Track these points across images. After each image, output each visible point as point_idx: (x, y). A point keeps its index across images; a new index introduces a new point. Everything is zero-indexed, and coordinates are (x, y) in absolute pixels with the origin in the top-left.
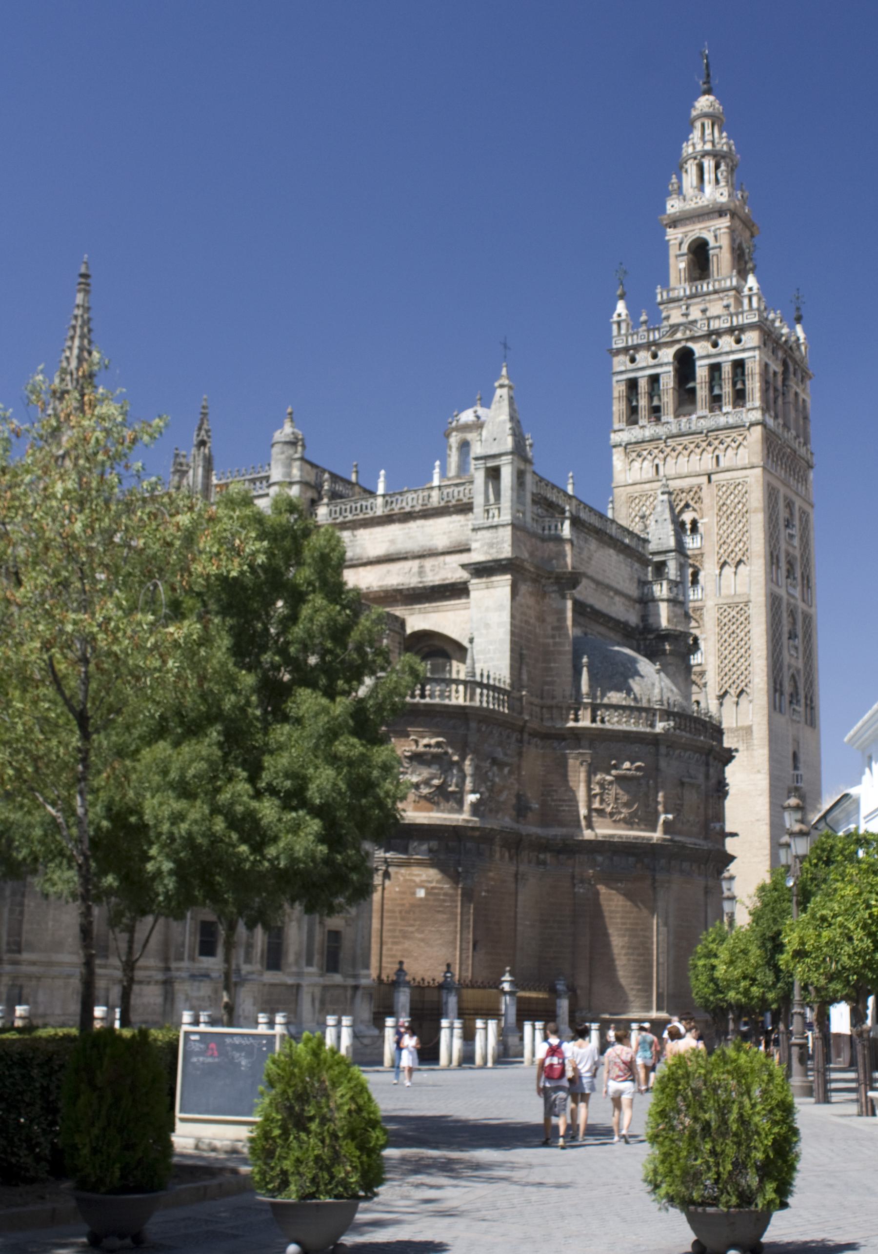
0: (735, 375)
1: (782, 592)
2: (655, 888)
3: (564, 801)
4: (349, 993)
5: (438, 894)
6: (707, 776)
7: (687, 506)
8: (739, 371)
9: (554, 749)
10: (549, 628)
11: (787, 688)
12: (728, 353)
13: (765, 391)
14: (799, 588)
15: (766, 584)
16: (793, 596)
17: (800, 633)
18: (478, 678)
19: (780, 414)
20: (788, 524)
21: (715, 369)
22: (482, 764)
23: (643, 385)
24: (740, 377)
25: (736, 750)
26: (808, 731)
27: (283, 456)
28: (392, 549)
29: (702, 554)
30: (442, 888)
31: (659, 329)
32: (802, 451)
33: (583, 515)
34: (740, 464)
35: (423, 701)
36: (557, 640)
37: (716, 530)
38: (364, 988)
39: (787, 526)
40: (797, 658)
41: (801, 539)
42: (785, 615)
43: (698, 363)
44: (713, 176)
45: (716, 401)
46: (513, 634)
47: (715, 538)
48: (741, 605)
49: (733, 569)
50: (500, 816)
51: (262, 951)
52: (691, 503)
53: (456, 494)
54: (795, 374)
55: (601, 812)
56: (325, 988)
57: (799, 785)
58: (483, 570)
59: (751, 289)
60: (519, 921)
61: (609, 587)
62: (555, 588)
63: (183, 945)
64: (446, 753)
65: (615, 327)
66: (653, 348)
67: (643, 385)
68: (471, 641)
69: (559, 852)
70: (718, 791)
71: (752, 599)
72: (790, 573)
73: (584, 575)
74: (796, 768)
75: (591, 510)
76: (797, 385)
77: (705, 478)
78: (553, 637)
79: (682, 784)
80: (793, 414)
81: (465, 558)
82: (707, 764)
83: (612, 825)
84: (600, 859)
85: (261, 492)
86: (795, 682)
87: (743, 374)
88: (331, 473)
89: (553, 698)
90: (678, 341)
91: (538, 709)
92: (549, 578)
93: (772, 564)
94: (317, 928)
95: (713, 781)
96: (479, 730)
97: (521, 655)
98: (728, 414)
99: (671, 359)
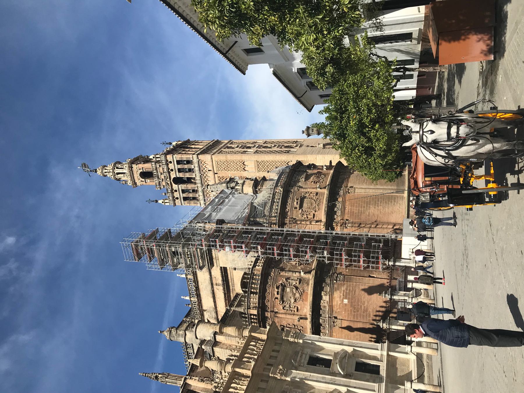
5: (346, 292)
18: (251, 267)
21: (180, 170)
23: (185, 195)
28: (211, 295)
30: (344, 291)
31: (167, 189)
37: (233, 172)
43: (178, 176)
45: (190, 170)
64: (281, 284)
65: (166, 204)
71: (256, 160)
82: (299, 171)
83: (321, 210)
85: (191, 345)
87: (181, 161)
98: (195, 166)
99: (177, 185)
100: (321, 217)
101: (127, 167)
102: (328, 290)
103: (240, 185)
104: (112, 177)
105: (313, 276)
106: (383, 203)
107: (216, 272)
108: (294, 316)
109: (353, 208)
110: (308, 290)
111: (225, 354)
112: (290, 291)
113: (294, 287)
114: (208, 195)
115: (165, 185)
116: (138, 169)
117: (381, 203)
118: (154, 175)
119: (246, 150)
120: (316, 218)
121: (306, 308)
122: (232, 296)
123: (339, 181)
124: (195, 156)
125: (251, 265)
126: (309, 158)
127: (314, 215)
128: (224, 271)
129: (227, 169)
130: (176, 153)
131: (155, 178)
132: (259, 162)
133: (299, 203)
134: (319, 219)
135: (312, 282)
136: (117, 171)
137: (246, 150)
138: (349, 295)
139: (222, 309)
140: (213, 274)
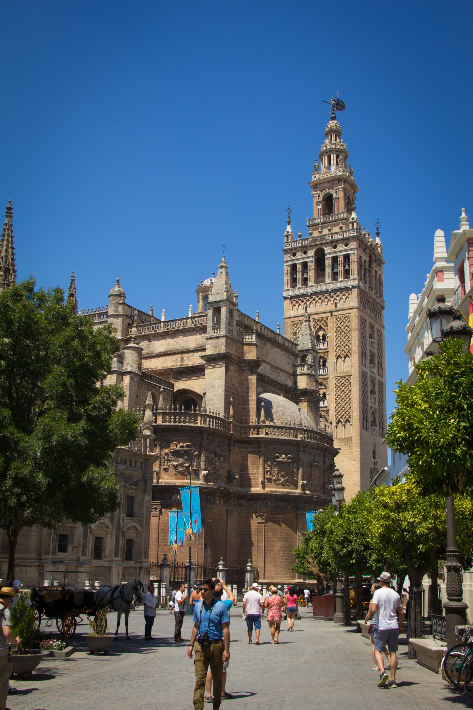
0: (345, 262)
1: (368, 370)
4: (138, 570)
6: (324, 462)
7: (321, 328)
8: (347, 260)
9: (247, 448)
11: (370, 418)
13: (360, 270)
14: (376, 369)
15: (359, 367)
16: (373, 373)
17: (377, 391)
18: (208, 413)
19: (367, 281)
20: (371, 337)
21: (335, 259)
22: (210, 456)
23: (299, 267)
24: (347, 263)
25: (340, 449)
27: (114, 302)
29: (328, 352)
32: (379, 300)
33: (264, 332)
34: (346, 306)
35: (180, 424)
37: (335, 340)
38: (145, 568)
39: (370, 338)
40: (375, 403)
41: (378, 344)
42: (369, 382)
44: (335, 162)
45: (335, 276)
46: (226, 390)
47: (334, 344)
49: (343, 359)
51: (92, 550)
52: (323, 326)
53: (200, 321)
54: (375, 262)
55: (270, 480)
56: (125, 568)
57: (376, 466)
59: (353, 219)
60: (228, 534)
62: (248, 368)
63: (49, 547)
65: (286, 238)
66: (304, 249)
68: (205, 394)
69: (249, 500)
70: (330, 469)
71: (352, 374)
72: (372, 361)
73: (264, 362)
74: (374, 458)
75: (268, 329)
76: (376, 267)
77: (329, 314)
79: (311, 466)
80: (374, 282)
81: (203, 354)
82: (324, 456)
83: (276, 486)
84: (269, 503)
86: (374, 415)
87: (349, 262)
88: (138, 311)
90: (317, 245)
91: (239, 429)
92: (245, 363)
93: (363, 356)
94: (121, 537)
95: (328, 464)
96: (208, 439)
98: (341, 283)
100: (269, 487)
103: (310, 371)
104: (324, 148)
106: (287, 556)
108: (159, 466)
117: (286, 554)
124: (356, 283)
136: (333, 156)
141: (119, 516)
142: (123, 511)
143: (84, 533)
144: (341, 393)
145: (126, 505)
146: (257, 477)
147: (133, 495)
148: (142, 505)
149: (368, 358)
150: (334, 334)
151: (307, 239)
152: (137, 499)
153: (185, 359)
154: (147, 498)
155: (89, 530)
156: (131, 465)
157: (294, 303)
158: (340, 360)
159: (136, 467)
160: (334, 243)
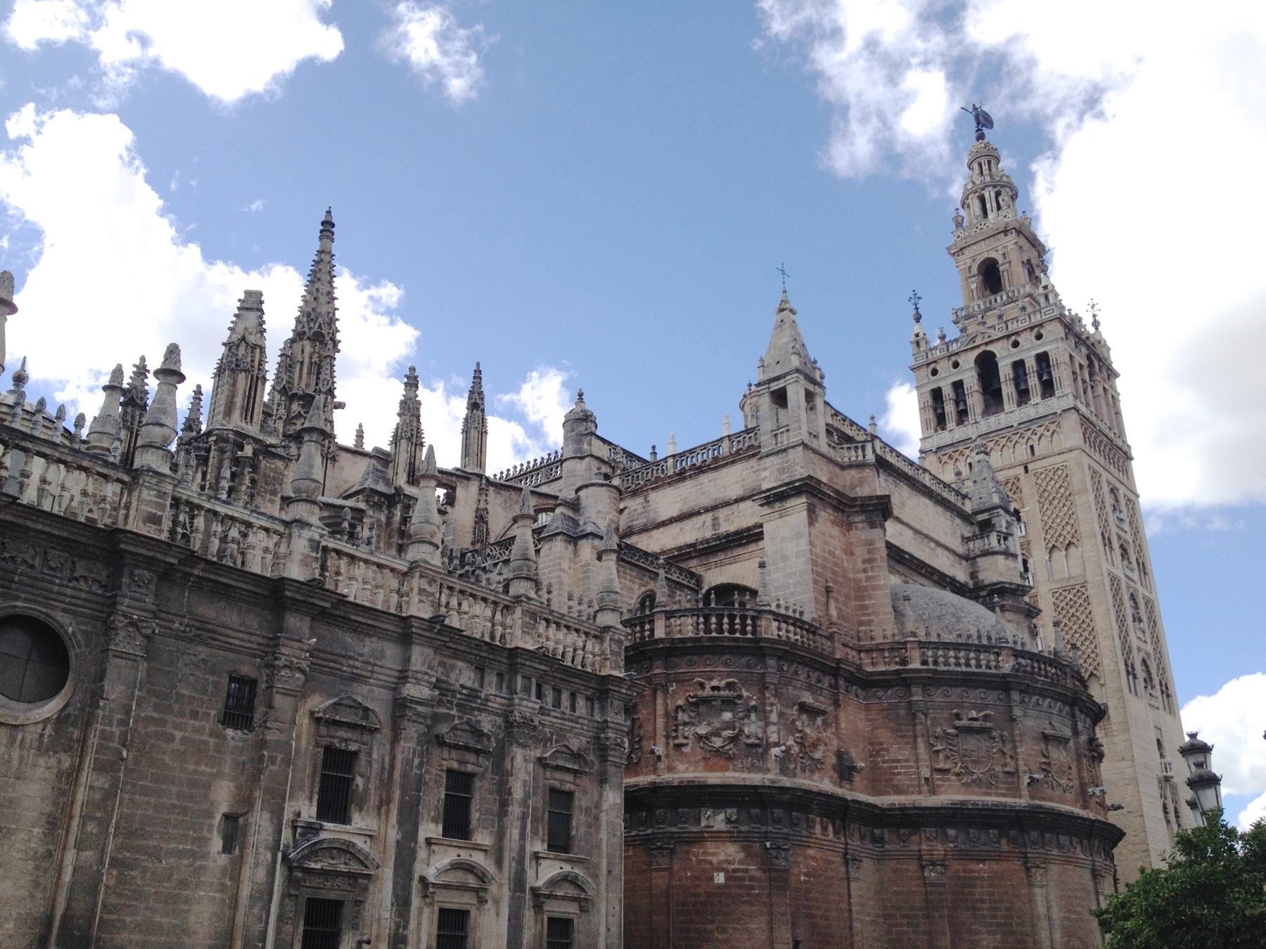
1: (1119, 573)
2: (1028, 869)
3: (898, 761)
5: (743, 879)
6: (1076, 733)
10: (859, 561)
11: (1141, 674)
12: (1028, 349)
14: (1136, 572)
16: (1131, 580)
17: (1145, 619)
19: (1092, 403)
21: (1019, 366)
22: (788, 711)
23: (948, 392)
26: (1168, 717)
28: (686, 509)
30: (746, 871)
32: (1118, 442)
34: (1056, 450)
36: (870, 574)
37: (1040, 517)
40: (1145, 642)
44: (994, 205)
47: (1040, 525)
48: (1077, 587)
50: (816, 776)
58: (775, 498)
61: (927, 536)
64: (740, 697)
66: (953, 358)
67: (948, 392)
71: (1089, 579)
77: (1022, 469)
78: (865, 571)
79: (1046, 738)
80: (1104, 408)
82: (1073, 716)
83: (963, 789)
84: (952, 832)
86: (1147, 667)
87: (1048, 366)
89: (872, 639)
90: (978, 346)
93: (1105, 545)
95: (1083, 738)
96: (780, 669)
97: (827, 587)
98: (1038, 405)
99: (972, 364)
101: (1006, 220)
102: (743, 828)
103: (1004, 546)
105: (773, 782)
107: (746, 516)
109: (985, 883)
110: (734, 770)
111: (550, 566)
112: (726, 722)
113: (737, 731)
114: (956, 455)
115: (969, 331)
116: (1005, 250)
118: (992, 298)
119: (1116, 545)
120: (938, 779)
121: (687, 769)
122: (693, 565)
123: (1061, 837)
124: (1070, 402)
125: (778, 606)
126: (1121, 736)
127: (947, 771)
128: (752, 535)
129: (1044, 498)
130: (1071, 347)
131: (985, 302)
132: (1083, 590)
133: (976, 724)
134: (939, 786)
135: (755, 778)
136: (989, 194)
137: (1116, 545)
138: (738, 887)
139: (654, 542)
140: (742, 505)
141: (522, 848)
142: (535, 832)
143: (395, 895)
144: (1069, 620)
145: (546, 816)
146: (911, 767)
147: (568, 787)
148: (597, 818)
149: (1118, 552)
150: (1038, 506)
151: (957, 340)
152: (581, 801)
153: (721, 521)
154: (611, 799)
155: (415, 884)
156: (557, 704)
157: (945, 459)
158: (1056, 554)
159: (573, 708)
160: (1013, 338)
